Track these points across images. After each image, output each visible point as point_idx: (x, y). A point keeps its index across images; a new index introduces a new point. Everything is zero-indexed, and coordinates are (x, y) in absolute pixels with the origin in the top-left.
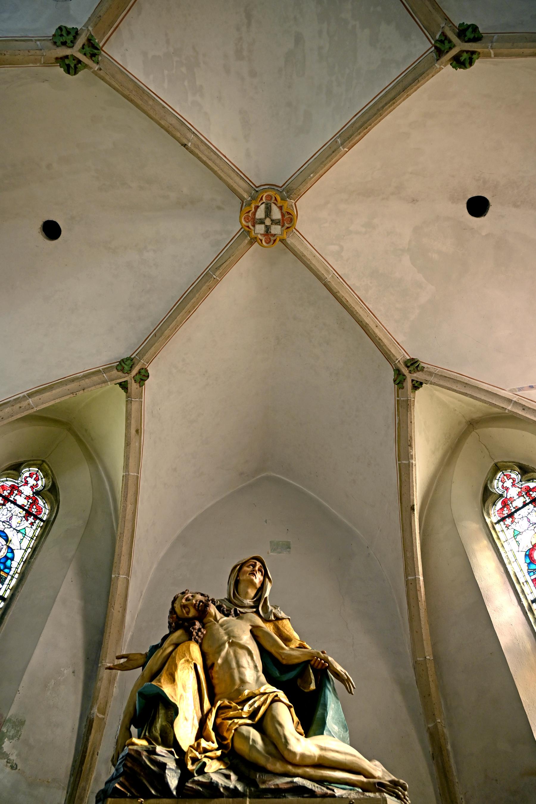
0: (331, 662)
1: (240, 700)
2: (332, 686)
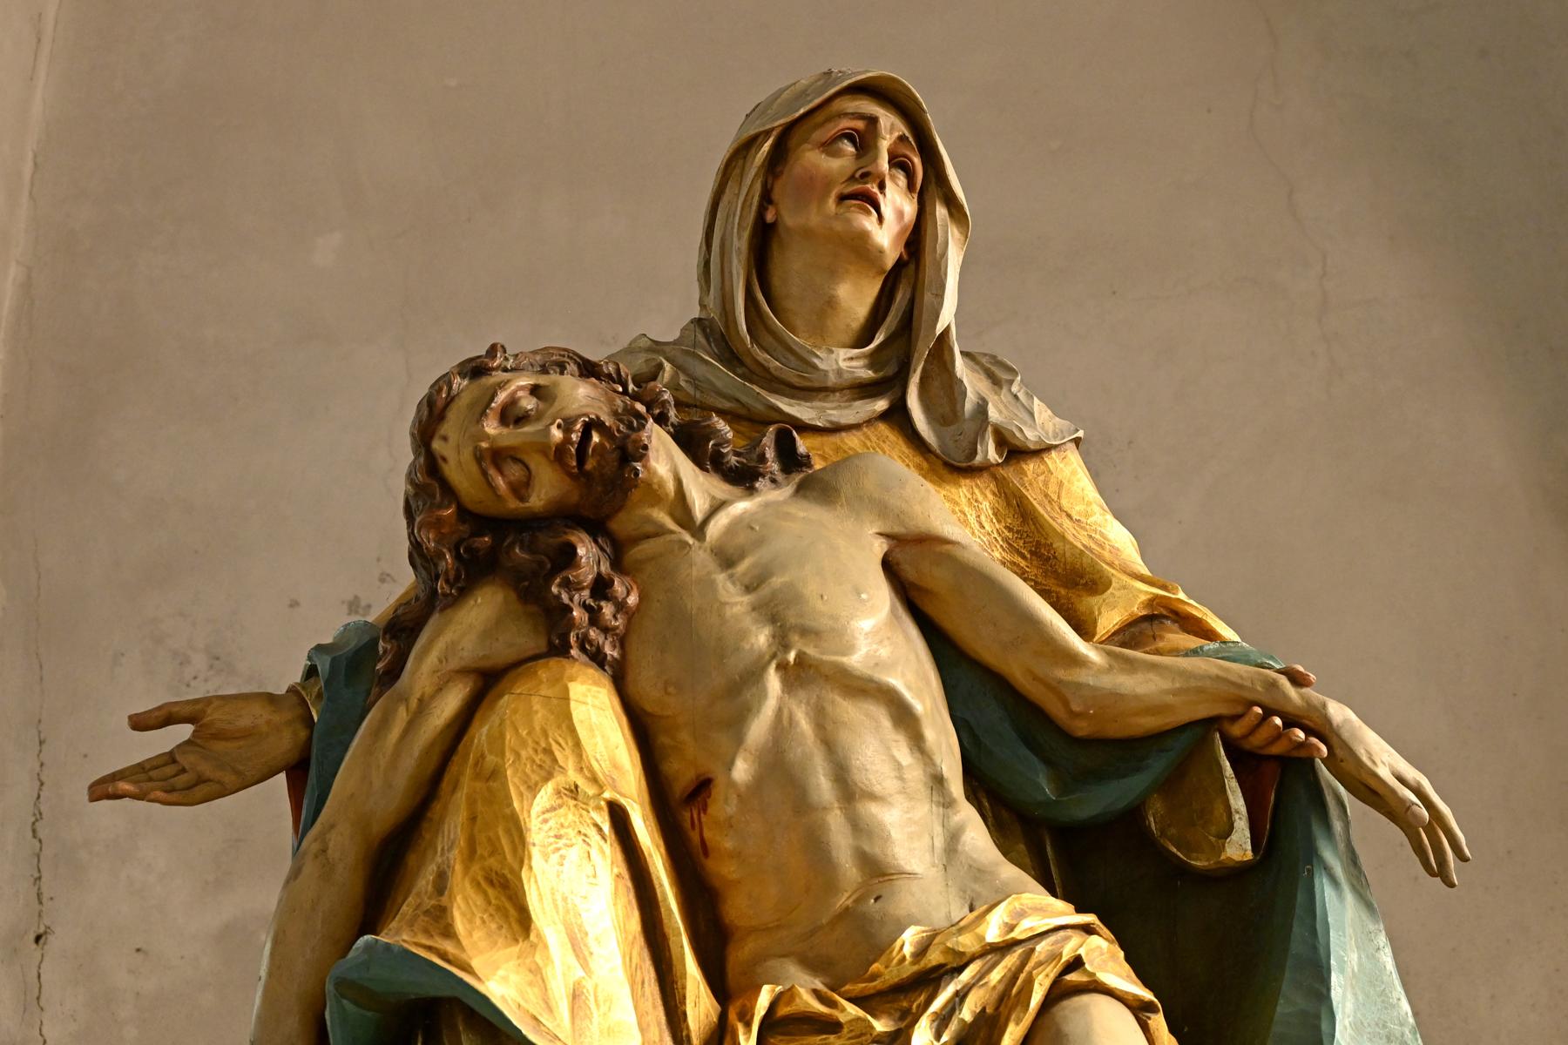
0: (1345, 735)
1: (877, 984)
2: (1342, 846)
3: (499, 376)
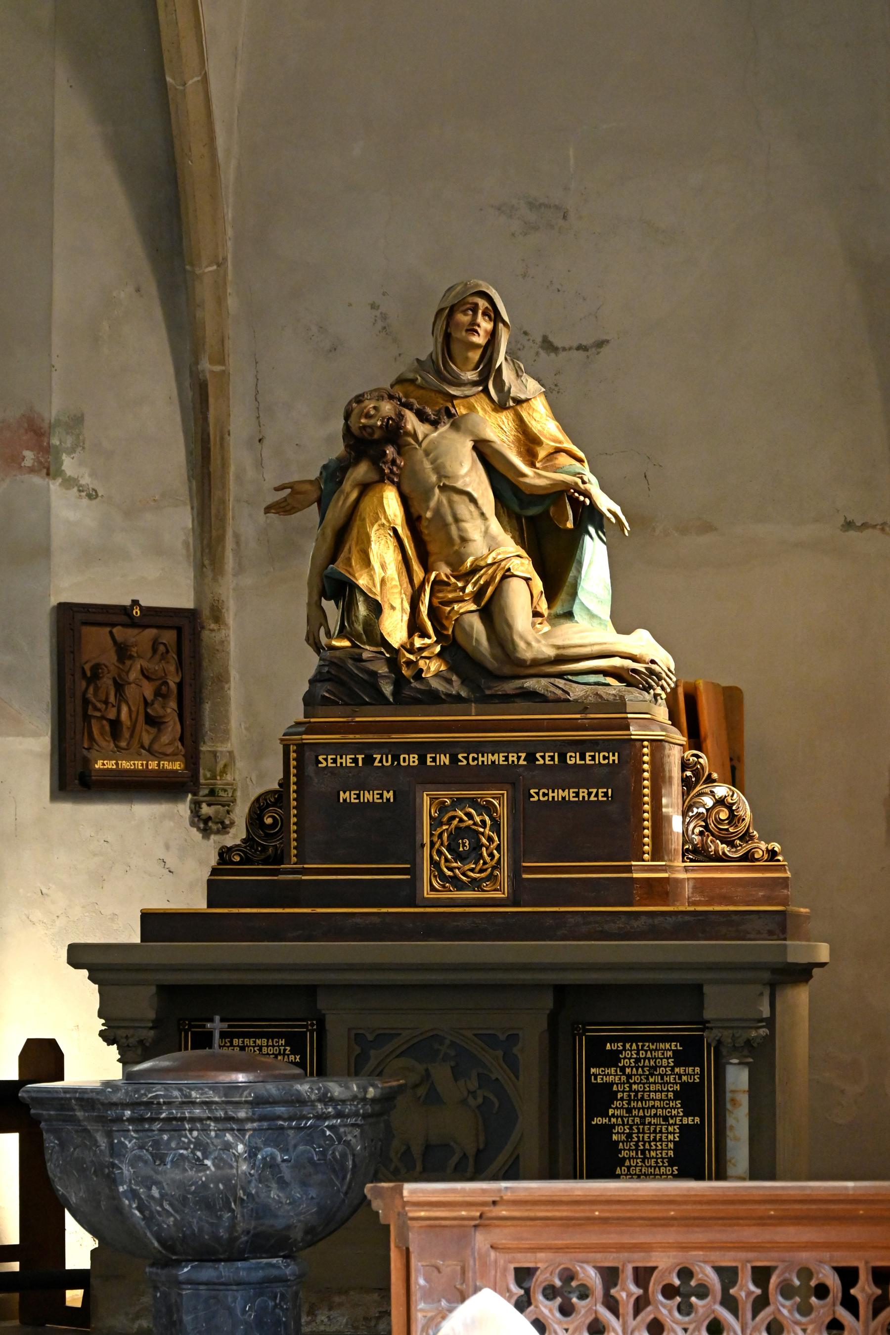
3: (367, 402)
